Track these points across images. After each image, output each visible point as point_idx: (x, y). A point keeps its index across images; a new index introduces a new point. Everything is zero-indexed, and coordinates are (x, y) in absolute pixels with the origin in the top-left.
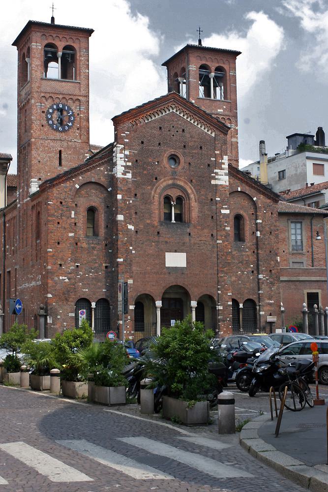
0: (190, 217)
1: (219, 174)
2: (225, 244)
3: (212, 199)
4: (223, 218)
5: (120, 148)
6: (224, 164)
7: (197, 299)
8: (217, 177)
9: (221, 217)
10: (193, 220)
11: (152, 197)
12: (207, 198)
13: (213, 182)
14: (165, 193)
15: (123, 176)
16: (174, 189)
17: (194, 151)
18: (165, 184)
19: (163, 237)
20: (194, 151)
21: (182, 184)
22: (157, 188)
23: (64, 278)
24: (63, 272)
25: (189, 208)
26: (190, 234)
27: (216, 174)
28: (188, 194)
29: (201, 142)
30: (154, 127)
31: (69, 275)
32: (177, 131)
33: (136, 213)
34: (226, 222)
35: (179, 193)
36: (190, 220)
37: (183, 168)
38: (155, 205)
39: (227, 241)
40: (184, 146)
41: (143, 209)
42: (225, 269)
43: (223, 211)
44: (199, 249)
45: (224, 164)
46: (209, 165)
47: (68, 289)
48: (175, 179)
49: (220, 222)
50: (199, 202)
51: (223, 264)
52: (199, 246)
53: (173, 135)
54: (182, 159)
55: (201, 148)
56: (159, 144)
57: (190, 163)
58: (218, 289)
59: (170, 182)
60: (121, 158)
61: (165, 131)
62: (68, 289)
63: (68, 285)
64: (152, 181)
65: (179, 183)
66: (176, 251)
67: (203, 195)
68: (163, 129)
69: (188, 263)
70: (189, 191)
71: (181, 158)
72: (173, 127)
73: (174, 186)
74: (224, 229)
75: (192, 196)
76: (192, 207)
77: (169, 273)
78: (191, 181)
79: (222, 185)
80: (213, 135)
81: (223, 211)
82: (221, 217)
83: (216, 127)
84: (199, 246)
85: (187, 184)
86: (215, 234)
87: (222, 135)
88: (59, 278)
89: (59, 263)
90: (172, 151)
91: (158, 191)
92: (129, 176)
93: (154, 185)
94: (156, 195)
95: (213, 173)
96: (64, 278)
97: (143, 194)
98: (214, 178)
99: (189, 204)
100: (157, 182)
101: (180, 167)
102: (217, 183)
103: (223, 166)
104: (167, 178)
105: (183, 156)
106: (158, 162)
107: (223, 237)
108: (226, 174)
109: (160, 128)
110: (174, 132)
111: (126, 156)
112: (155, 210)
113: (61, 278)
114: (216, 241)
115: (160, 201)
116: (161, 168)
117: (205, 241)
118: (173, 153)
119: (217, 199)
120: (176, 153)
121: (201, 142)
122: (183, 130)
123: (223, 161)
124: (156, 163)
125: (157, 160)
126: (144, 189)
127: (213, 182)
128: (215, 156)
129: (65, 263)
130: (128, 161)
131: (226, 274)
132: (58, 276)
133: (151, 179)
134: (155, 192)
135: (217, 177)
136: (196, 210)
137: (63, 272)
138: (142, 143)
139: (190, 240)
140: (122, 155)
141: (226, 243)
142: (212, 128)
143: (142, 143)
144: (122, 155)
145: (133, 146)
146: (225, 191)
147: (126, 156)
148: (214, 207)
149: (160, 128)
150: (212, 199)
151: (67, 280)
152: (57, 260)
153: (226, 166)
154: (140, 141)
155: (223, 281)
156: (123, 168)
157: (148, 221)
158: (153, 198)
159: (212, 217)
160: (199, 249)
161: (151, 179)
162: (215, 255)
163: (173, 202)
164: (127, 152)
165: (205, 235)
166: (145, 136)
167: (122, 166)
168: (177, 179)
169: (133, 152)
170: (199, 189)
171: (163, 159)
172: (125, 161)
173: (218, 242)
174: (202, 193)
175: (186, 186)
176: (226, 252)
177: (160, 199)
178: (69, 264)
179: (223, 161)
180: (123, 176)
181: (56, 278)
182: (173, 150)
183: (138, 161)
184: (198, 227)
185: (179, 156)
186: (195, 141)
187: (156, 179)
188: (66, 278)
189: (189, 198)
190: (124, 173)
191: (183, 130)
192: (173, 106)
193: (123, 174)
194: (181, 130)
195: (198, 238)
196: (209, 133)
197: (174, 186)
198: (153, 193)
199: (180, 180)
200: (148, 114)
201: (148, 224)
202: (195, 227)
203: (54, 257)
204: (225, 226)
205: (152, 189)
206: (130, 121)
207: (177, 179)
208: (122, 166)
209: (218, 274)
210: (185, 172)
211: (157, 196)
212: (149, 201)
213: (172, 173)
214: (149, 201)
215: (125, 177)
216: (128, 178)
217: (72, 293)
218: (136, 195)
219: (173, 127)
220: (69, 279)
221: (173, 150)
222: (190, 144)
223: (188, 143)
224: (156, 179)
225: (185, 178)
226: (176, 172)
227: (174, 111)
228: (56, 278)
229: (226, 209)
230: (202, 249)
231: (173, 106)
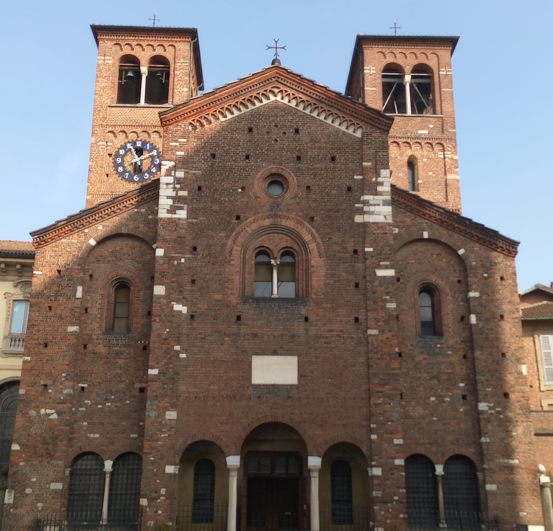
0: (307, 286)
1: (371, 202)
2: (386, 336)
3: (355, 252)
4: (381, 285)
5: (167, 167)
6: (381, 184)
7: (322, 452)
8: (366, 209)
9: (377, 283)
10: (314, 291)
11: (227, 251)
12: (346, 248)
13: (358, 219)
14: (257, 243)
15: (169, 216)
16: (276, 235)
17: (318, 166)
18: (255, 226)
19: (247, 324)
20: (318, 166)
21: (290, 224)
22: (238, 234)
23: (48, 411)
24: (49, 400)
25: (307, 269)
26: (306, 319)
27: (366, 203)
28: (304, 244)
29: (332, 149)
30: (238, 129)
31: (61, 406)
32: (284, 133)
33: (193, 282)
34: (387, 293)
35: (283, 241)
36: (307, 291)
37: (295, 197)
38: (233, 265)
39: (390, 331)
40: (299, 158)
41: (208, 274)
42: (387, 387)
43: (380, 273)
44: (327, 348)
45: (381, 184)
46: (349, 189)
47: (56, 433)
48: (276, 216)
49: (374, 293)
50: (327, 257)
51: (381, 377)
52: (325, 343)
53: (276, 140)
54: (293, 180)
55: (333, 159)
56: (247, 157)
57: (308, 188)
58: (371, 431)
59: (267, 222)
60: (167, 184)
61: (258, 133)
62: (56, 433)
63: (56, 425)
64: (229, 223)
65: (285, 223)
66: (275, 353)
67: (335, 243)
68: (255, 132)
69: (301, 376)
70: (307, 237)
71: (290, 179)
72: (276, 126)
73: (275, 229)
74: (384, 307)
75: (312, 246)
76: (313, 267)
77: (259, 397)
78: (312, 218)
79: (377, 223)
80: (358, 134)
81: (380, 273)
82: (377, 283)
83: (365, 119)
84: (325, 343)
85: (301, 224)
86: (361, 317)
87: (377, 134)
88: (38, 413)
89: (42, 383)
90: (273, 168)
91: (241, 239)
92: (182, 214)
93: (233, 229)
94: (235, 248)
95: (359, 202)
96: (48, 411)
97: (210, 246)
98: (361, 212)
99: (307, 261)
100: (238, 224)
101: (288, 196)
102: (366, 220)
103: (380, 189)
104: (260, 215)
105: (296, 175)
106: (243, 188)
107: (381, 323)
108: (385, 203)
109: (250, 130)
110: (278, 134)
111: (178, 180)
112: (232, 275)
113: (43, 411)
114: (366, 331)
115: (244, 258)
116: (249, 197)
117: (341, 331)
118: (274, 171)
119: (367, 249)
120: (280, 171)
121: (332, 149)
122: (297, 131)
123: (380, 179)
124: (240, 190)
125: (241, 185)
126: (213, 236)
127: (358, 219)
128: (363, 171)
129: (54, 381)
130: (181, 189)
131: (389, 398)
132: (37, 408)
133: (228, 219)
134: (235, 240)
135: (366, 209)
136: (322, 272)
137: (48, 400)
138: (213, 156)
139: (307, 330)
140: (170, 180)
141: (389, 335)
142: (355, 122)
143: (213, 156)
144: (170, 180)
145: (194, 163)
146: (386, 233)
147: (178, 180)
148: (360, 266)
149: (250, 130)
150: (355, 252)
151: (54, 416)
152: (38, 376)
153: (386, 188)
154: (209, 154)
155: (381, 414)
156: (170, 202)
157: (218, 297)
158: (231, 253)
159: (357, 285)
160: (327, 348)
161: (228, 219)
162: (362, 360)
163: (275, 259)
164: (180, 174)
165: (341, 321)
166: (218, 145)
167: (168, 197)
168: (280, 216)
169: (194, 174)
170: (328, 234)
171: (253, 184)
172: (174, 188)
173: (371, 332)
174: (334, 240)
175: (300, 227)
176: (389, 354)
177: (245, 254)
178: (61, 384)
179: (380, 179)
180: (169, 216)
181: (33, 413)
182: (274, 166)
183: (203, 189)
184: (325, 305)
185: (287, 175)
186: (320, 148)
187: (238, 218)
188: (53, 411)
189: (306, 249)
190: (172, 210)
191: (297, 131)
192: (276, 90)
193: (169, 212)
194: (292, 130)
195: (325, 325)
196: (350, 131)
197: (275, 229)
198: (230, 243)
199: (288, 218)
200: (226, 106)
201: (217, 301)
202: (318, 304)
203: (34, 372)
204: (386, 301)
205: (227, 237)
206: (190, 121)
207: (280, 216)
208: (168, 197)
209: (370, 399)
210: (298, 203)
211: (239, 248)
212: (221, 258)
213: (270, 206)
214: (221, 258)
215: (174, 216)
216: (179, 219)
217: (61, 440)
218: (195, 249)
219: (276, 126)
220: (59, 413)
221: (274, 166)
222: (309, 153)
223: (307, 152)
224: (238, 218)
225: (297, 214)
226: (278, 205)
227: (279, 98)
228: (33, 413)
229: (387, 267)
230: (334, 348)
231: (276, 90)
